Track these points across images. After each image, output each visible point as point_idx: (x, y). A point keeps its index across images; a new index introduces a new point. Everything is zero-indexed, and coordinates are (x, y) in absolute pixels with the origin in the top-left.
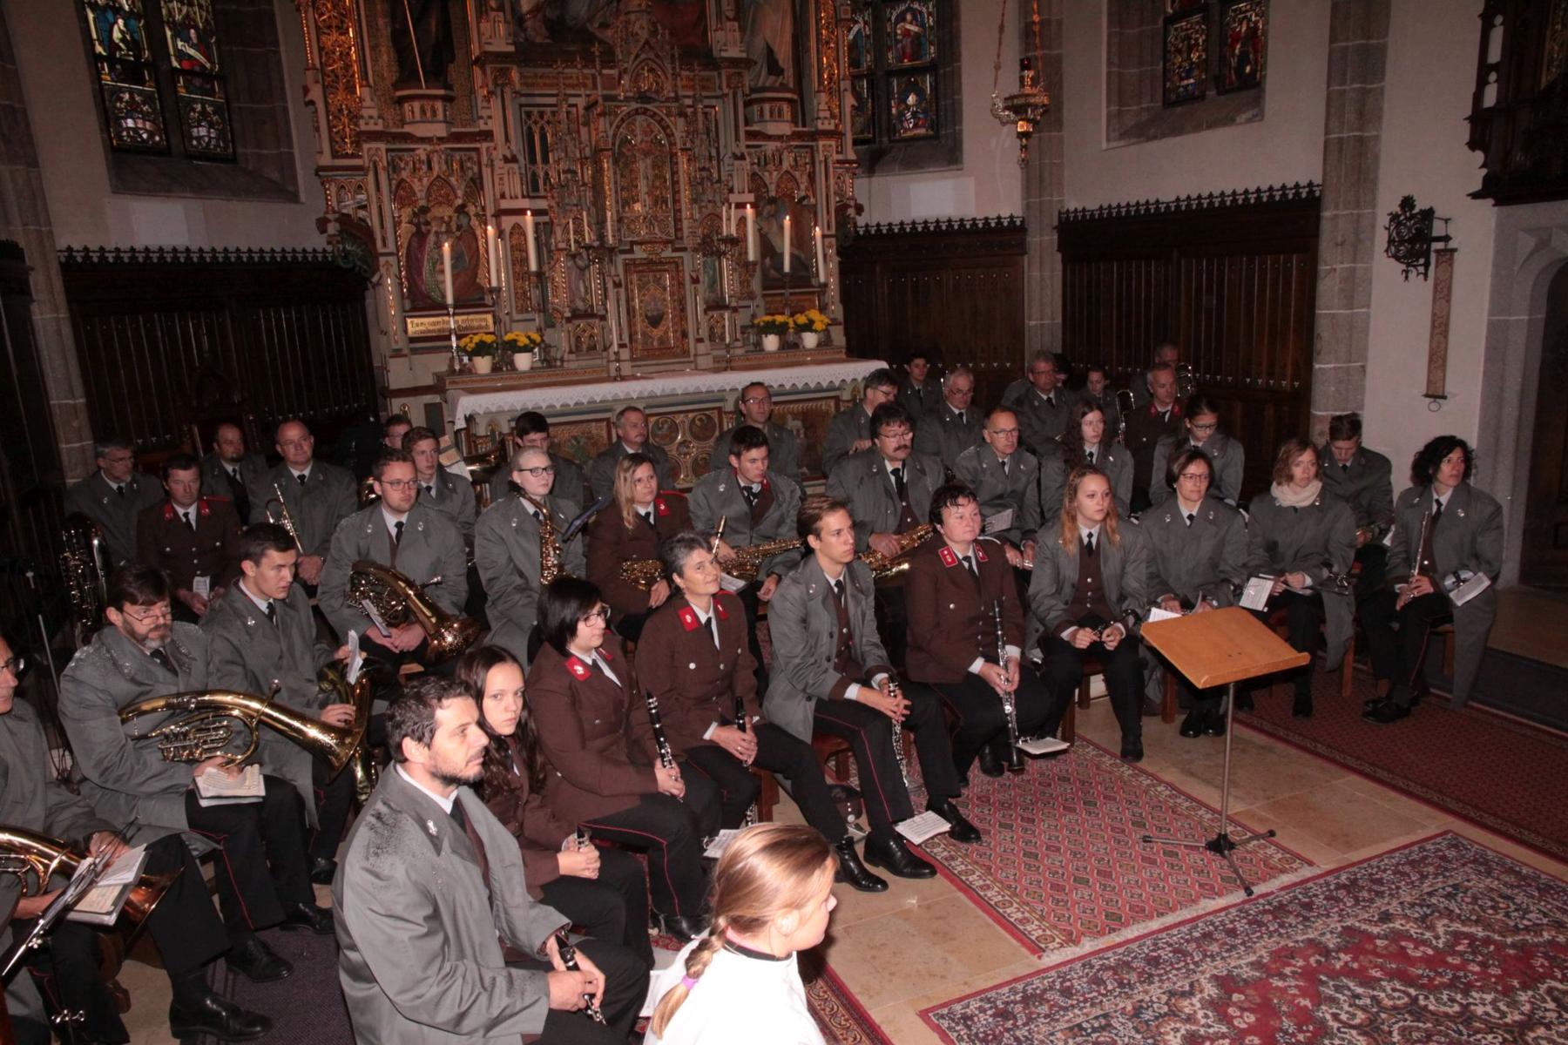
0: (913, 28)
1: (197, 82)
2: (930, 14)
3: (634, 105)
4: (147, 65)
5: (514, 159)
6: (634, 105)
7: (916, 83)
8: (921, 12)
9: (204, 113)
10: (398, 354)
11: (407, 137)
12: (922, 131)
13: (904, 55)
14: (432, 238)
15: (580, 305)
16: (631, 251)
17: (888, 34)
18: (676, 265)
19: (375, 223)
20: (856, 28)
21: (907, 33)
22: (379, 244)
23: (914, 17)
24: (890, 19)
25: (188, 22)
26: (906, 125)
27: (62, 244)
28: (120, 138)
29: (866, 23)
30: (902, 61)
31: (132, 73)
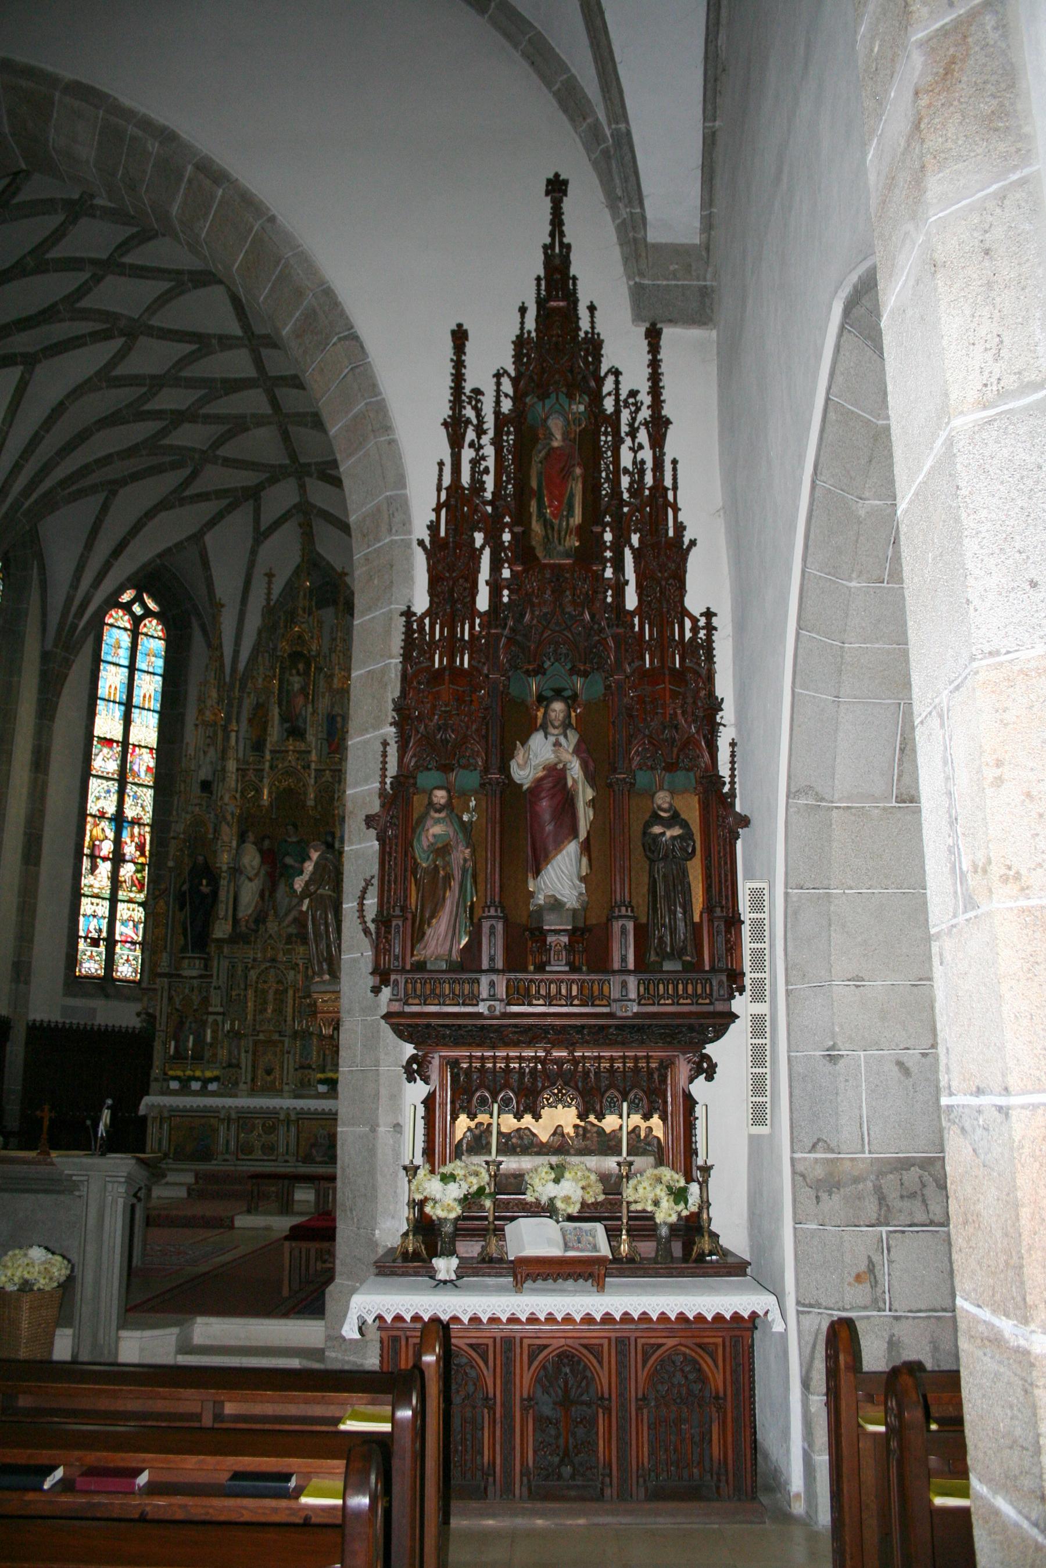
1: (128, 945)
3: (268, 964)
4: (104, 939)
5: (219, 988)
6: (268, 964)
9: (128, 960)
10: (156, 1080)
11: (179, 976)
14: (188, 1024)
15: (234, 1061)
16: (257, 1035)
18: (283, 1042)
19: (158, 1014)
22: (158, 1026)
25: (130, 919)
27: (31, 1017)
28: (80, 971)
31: (95, 943)
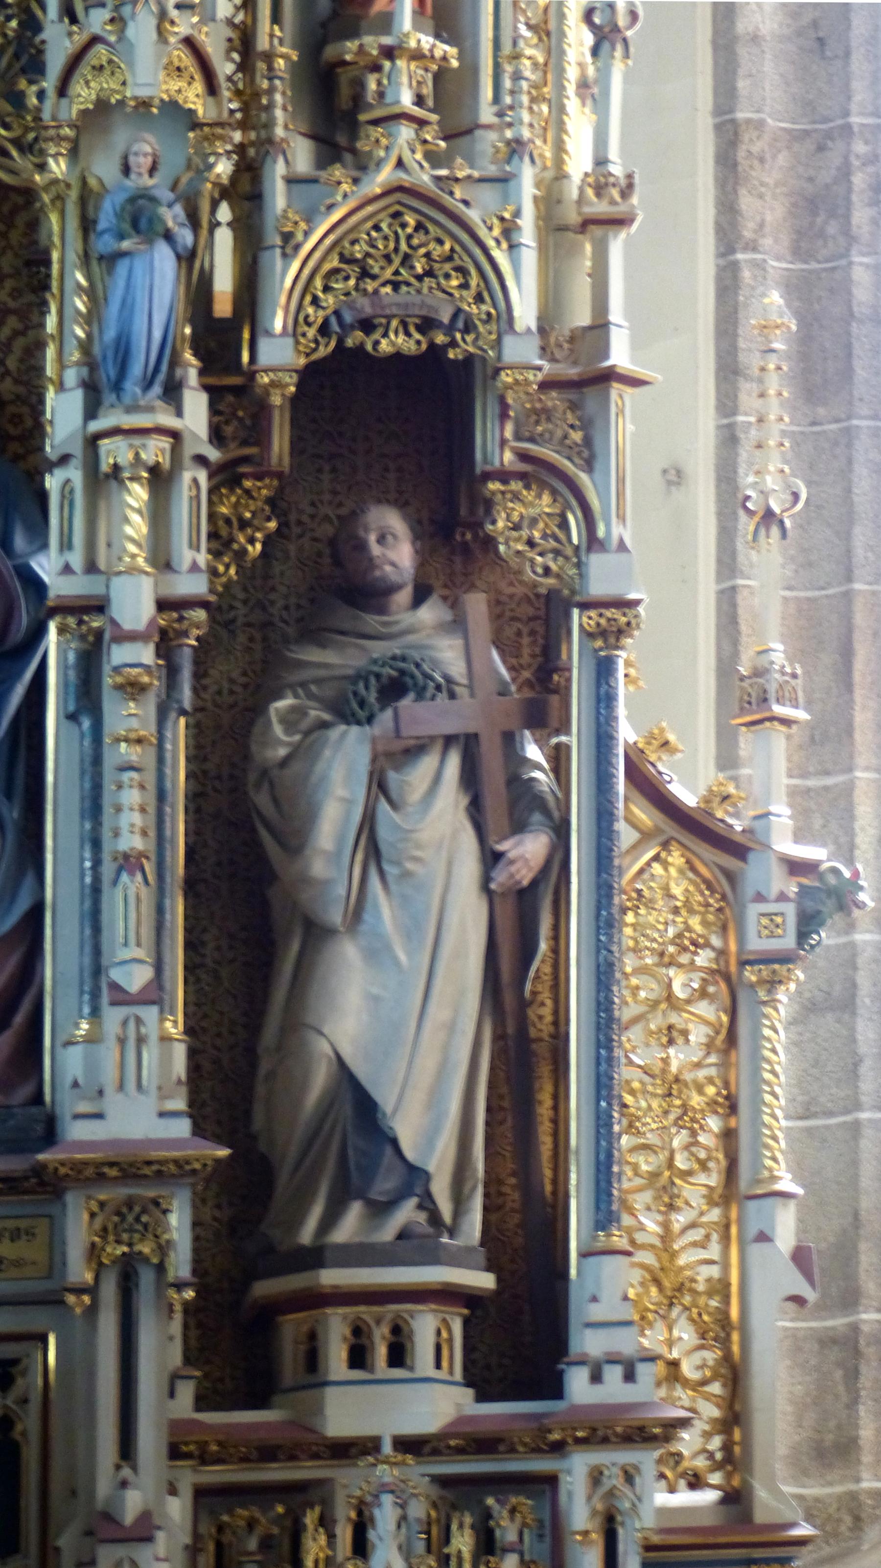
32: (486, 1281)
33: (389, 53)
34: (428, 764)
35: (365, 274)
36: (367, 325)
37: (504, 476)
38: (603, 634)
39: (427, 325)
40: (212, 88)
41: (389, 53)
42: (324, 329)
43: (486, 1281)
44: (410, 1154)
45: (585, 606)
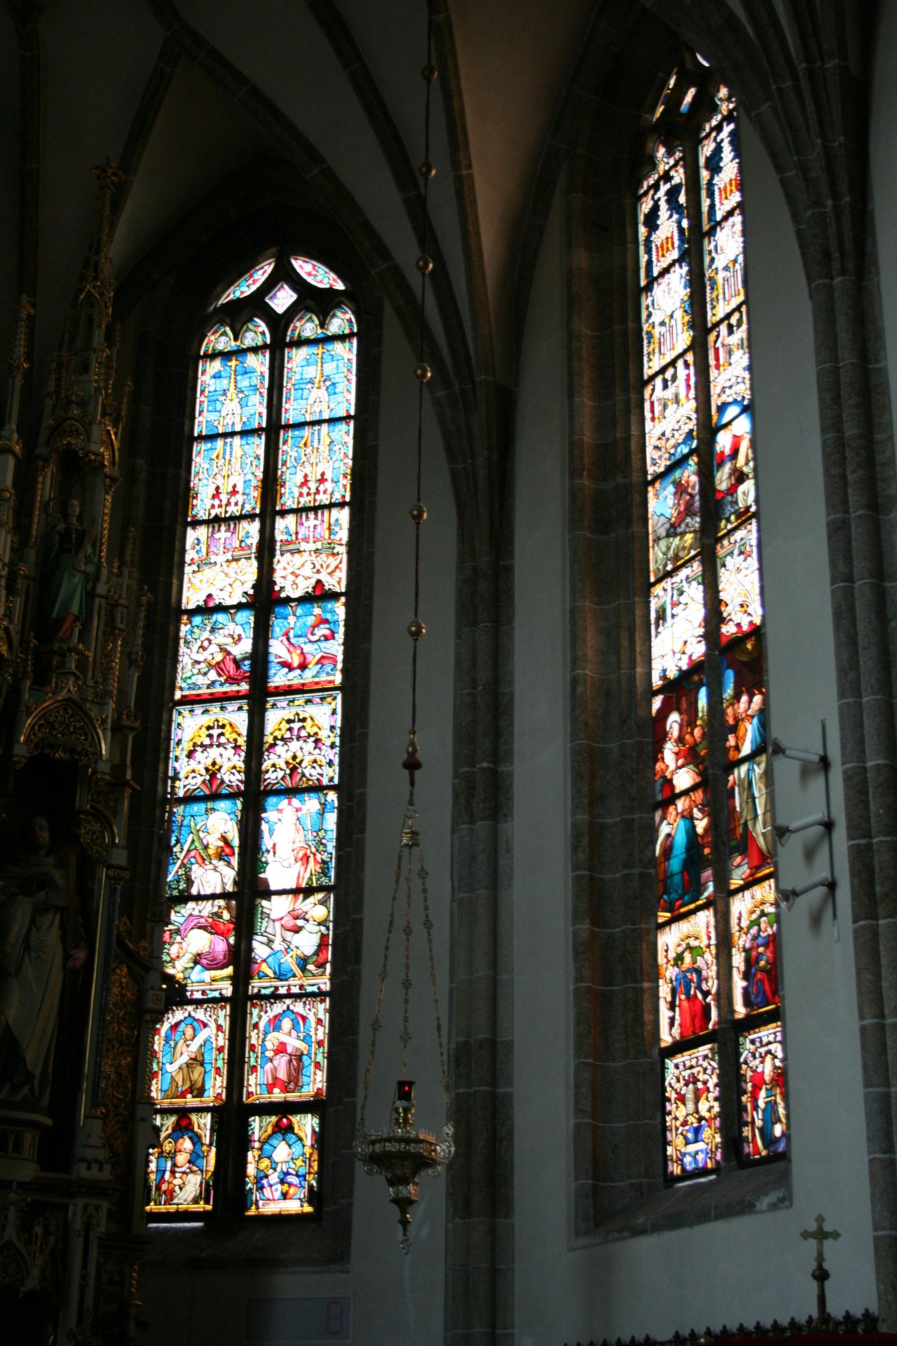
0: (294, 1043)
2: (319, 1022)
7: (290, 1128)
8: (304, 1018)
12: (293, 1206)
13: (275, 1083)
17: (253, 1048)
20: (203, 1035)
21: (281, 1049)
23: (294, 1027)
24: (256, 1026)
26: (267, 1192)
29: (219, 1028)
30: (270, 1091)
32: (49, 1122)
33: (70, 650)
34: (50, 916)
35: (53, 728)
36: (52, 747)
37: (86, 813)
38: (114, 878)
39: (72, 751)
40: (10, 648)
41: (70, 650)
42: (36, 746)
43: (49, 1122)
44: (29, 1068)
45: (109, 867)
